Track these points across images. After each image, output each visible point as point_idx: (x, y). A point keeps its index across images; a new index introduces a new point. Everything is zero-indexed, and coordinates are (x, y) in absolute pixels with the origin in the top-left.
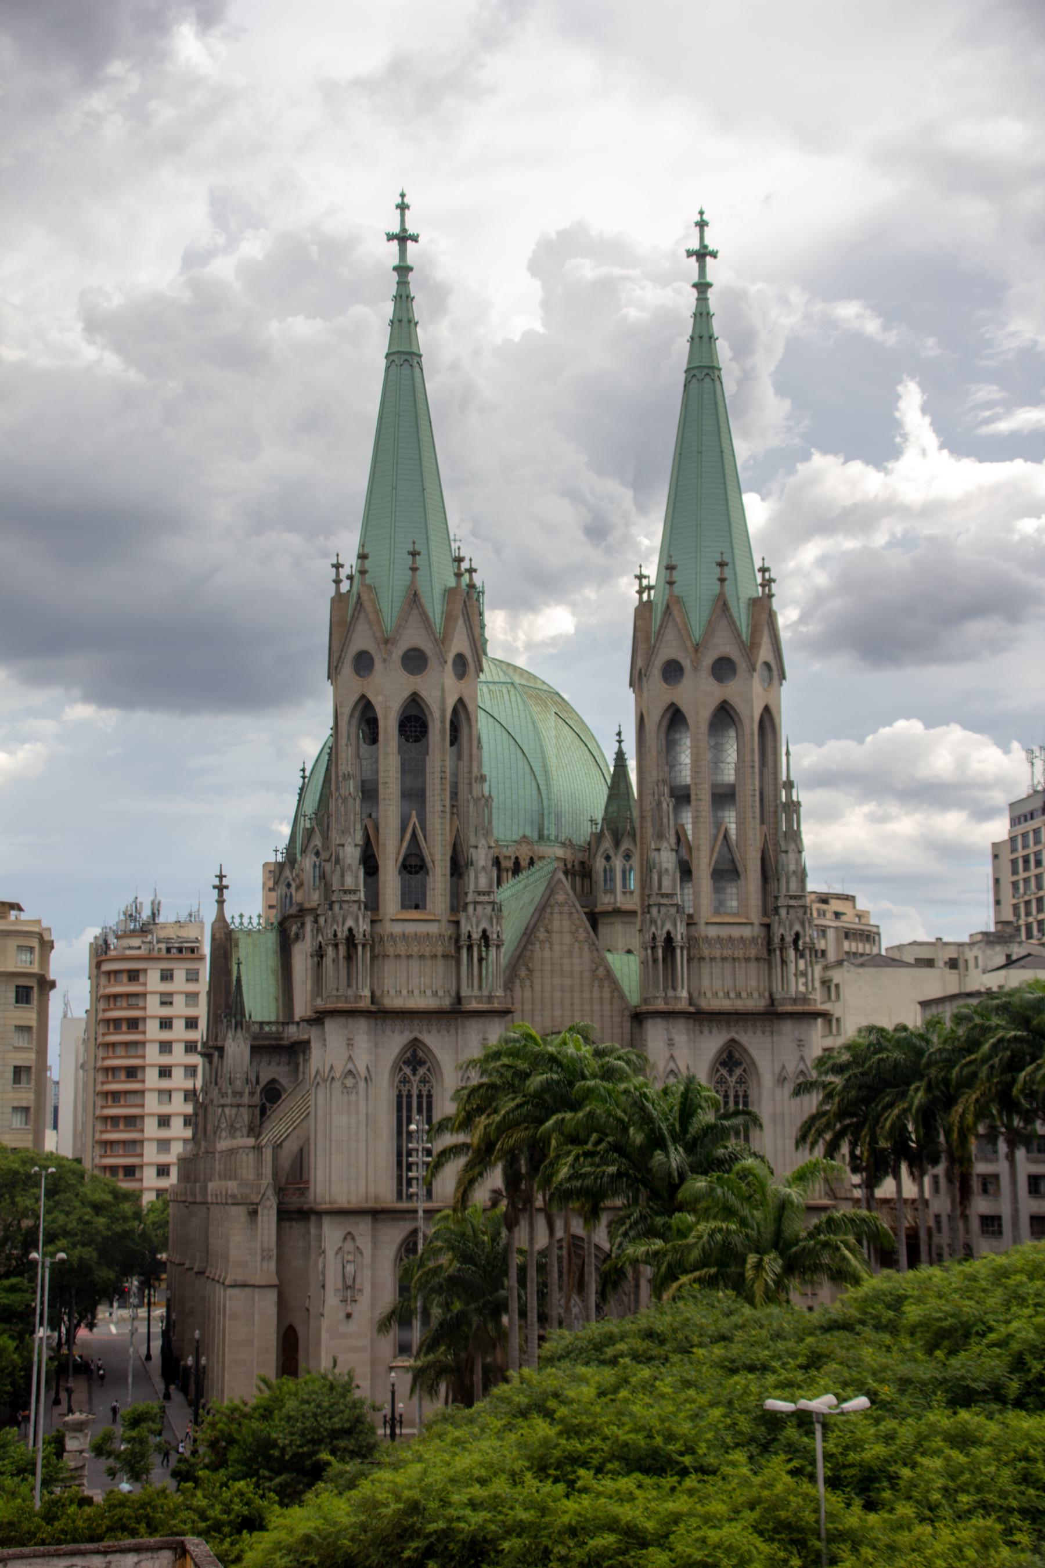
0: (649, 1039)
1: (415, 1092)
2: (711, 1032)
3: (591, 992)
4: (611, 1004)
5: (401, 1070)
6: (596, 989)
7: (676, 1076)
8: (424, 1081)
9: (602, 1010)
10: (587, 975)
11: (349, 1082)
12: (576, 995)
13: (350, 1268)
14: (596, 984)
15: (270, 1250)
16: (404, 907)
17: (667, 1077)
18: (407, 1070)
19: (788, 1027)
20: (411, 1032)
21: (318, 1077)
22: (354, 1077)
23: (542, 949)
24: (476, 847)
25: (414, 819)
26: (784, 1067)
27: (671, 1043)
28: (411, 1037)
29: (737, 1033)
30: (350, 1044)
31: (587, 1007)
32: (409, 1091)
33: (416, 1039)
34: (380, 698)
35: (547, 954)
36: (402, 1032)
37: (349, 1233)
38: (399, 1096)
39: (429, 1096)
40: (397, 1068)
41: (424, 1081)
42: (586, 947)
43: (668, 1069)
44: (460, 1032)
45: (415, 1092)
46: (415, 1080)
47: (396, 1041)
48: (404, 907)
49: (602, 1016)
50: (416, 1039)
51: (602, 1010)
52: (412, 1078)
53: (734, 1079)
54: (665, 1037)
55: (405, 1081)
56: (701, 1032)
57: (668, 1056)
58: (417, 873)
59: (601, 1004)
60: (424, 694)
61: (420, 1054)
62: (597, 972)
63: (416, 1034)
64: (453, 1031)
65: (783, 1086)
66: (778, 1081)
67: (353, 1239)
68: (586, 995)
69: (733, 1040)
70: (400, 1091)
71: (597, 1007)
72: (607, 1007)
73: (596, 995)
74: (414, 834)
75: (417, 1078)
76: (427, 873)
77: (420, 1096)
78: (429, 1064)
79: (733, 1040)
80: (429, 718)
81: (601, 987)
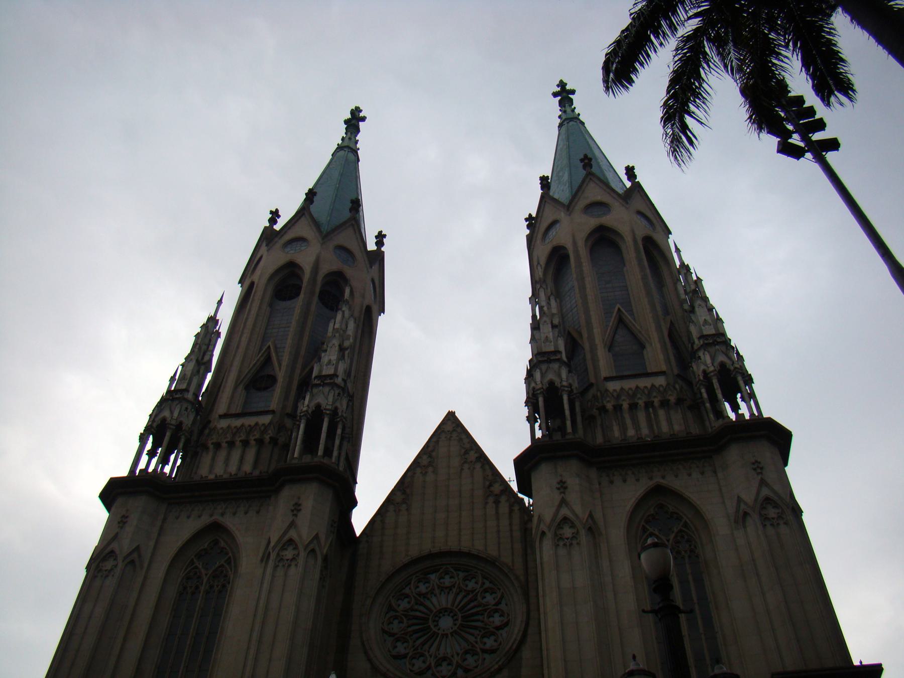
2: (625, 481)
3: (485, 508)
4: (510, 517)
5: (192, 562)
7: (573, 526)
9: (498, 526)
14: (491, 500)
17: (560, 526)
20: (211, 515)
23: (425, 474)
24: (326, 351)
26: (739, 500)
27: (562, 487)
29: (663, 477)
32: (197, 587)
33: (216, 528)
35: (430, 477)
36: (200, 517)
42: (478, 466)
43: (560, 517)
49: (498, 531)
50: (216, 528)
51: (498, 526)
52: (203, 571)
53: (672, 537)
56: (612, 482)
59: (498, 519)
61: (222, 544)
62: (492, 489)
65: (745, 527)
66: (736, 522)
69: (658, 490)
70: (185, 588)
75: (210, 572)
78: (230, 554)
79: (658, 490)
81: (497, 502)
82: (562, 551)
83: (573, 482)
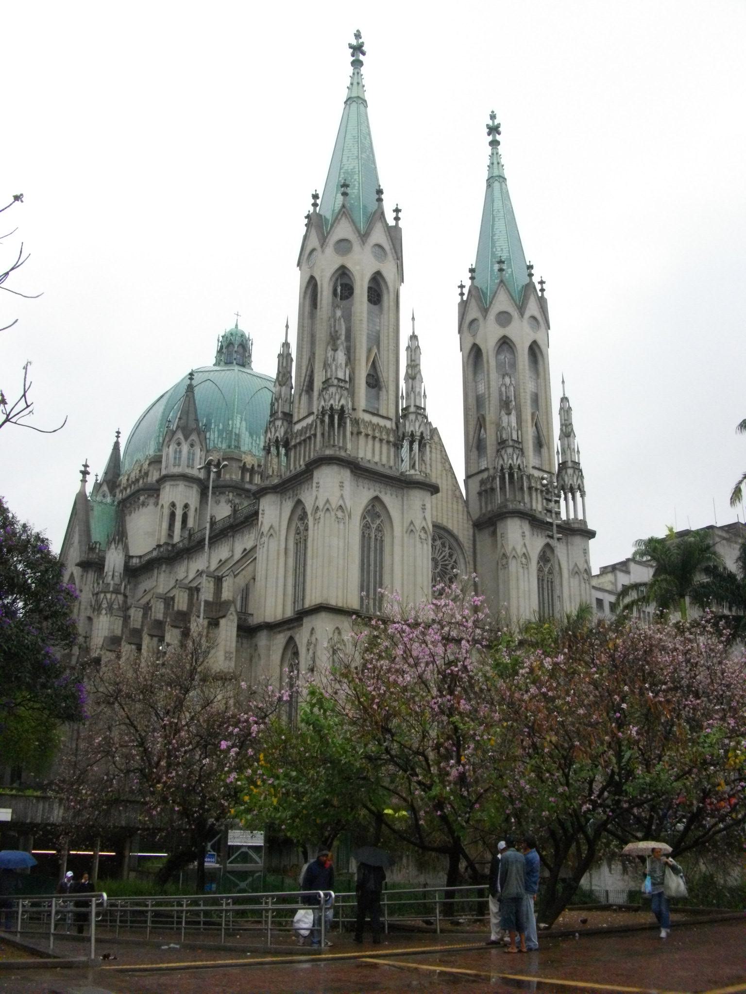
0: (509, 531)
1: (373, 536)
6: (455, 503)
10: (450, 492)
11: (340, 514)
12: (445, 504)
15: (232, 653)
18: (369, 519)
19: (577, 540)
21: (272, 531)
22: (343, 512)
25: (375, 350)
28: (375, 494)
30: (342, 486)
31: (450, 514)
33: (377, 498)
34: (358, 267)
37: (337, 628)
38: (363, 536)
39: (382, 541)
40: (364, 517)
41: (379, 529)
44: (405, 498)
45: (373, 536)
47: (365, 494)
50: (377, 498)
54: (520, 531)
57: (522, 543)
58: (373, 387)
60: (385, 274)
63: (376, 493)
64: (400, 498)
67: (340, 633)
68: (450, 505)
71: (455, 515)
72: (461, 516)
73: (455, 506)
74: (374, 362)
76: (380, 389)
77: (376, 539)
80: (385, 291)
82: (521, 570)
83: (527, 533)
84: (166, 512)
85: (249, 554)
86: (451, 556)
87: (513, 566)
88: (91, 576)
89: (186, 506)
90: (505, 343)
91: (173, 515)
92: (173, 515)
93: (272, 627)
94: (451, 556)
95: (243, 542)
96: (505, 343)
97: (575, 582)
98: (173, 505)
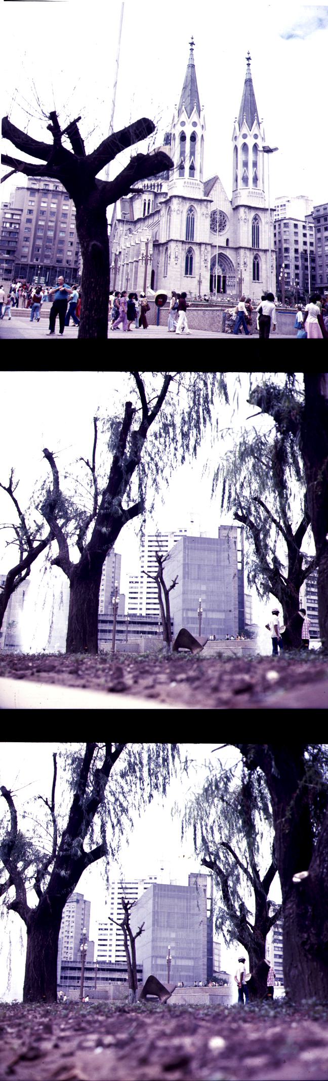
8: (193, 215)
13: (177, 253)
16: (190, 176)
25: (193, 157)
41: (193, 215)
46: (191, 214)
48: (190, 176)
55: (188, 214)
84: (143, 202)
85: (158, 222)
86: (224, 219)
87: (242, 223)
88: (121, 224)
89: (149, 200)
90: (245, 146)
91: (145, 203)
92: (145, 203)
93: (163, 244)
94: (224, 219)
95: (156, 218)
96: (245, 146)
97: (267, 226)
98: (145, 200)
